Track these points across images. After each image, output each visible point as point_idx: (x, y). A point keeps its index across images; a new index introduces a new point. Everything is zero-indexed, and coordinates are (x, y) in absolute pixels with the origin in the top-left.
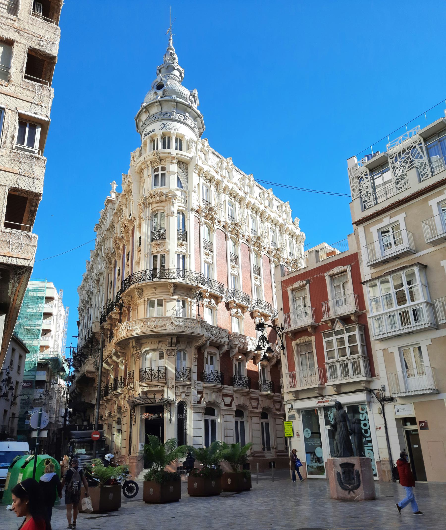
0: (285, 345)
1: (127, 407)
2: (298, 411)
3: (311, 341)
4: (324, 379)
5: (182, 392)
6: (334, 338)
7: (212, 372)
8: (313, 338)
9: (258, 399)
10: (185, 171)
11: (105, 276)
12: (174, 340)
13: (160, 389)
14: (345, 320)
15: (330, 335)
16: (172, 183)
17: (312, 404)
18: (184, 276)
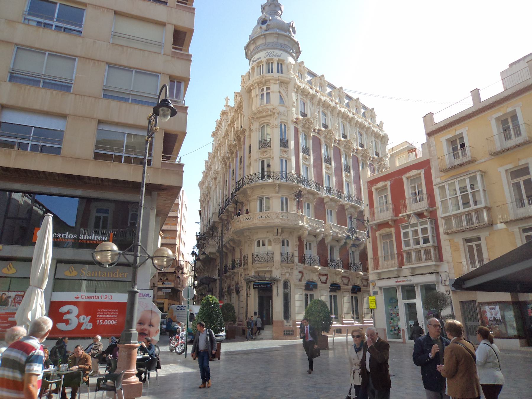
0: (370, 235)
1: (244, 284)
2: (380, 288)
3: (391, 232)
4: (401, 264)
5: (287, 272)
6: (410, 230)
8: (393, 230)
9: (348, 278)
14: (420, 215)
15: (406, 227)
16: (274, 99)
17: (391, 283)
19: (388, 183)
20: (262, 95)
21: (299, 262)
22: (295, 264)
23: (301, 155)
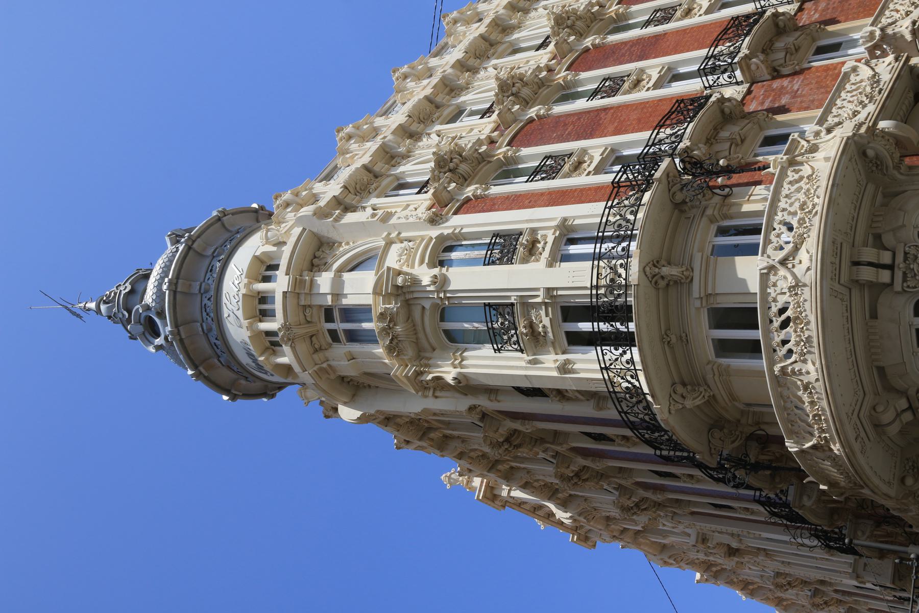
11: (714, 527)
20: (353, 336)
23: (558, 183)
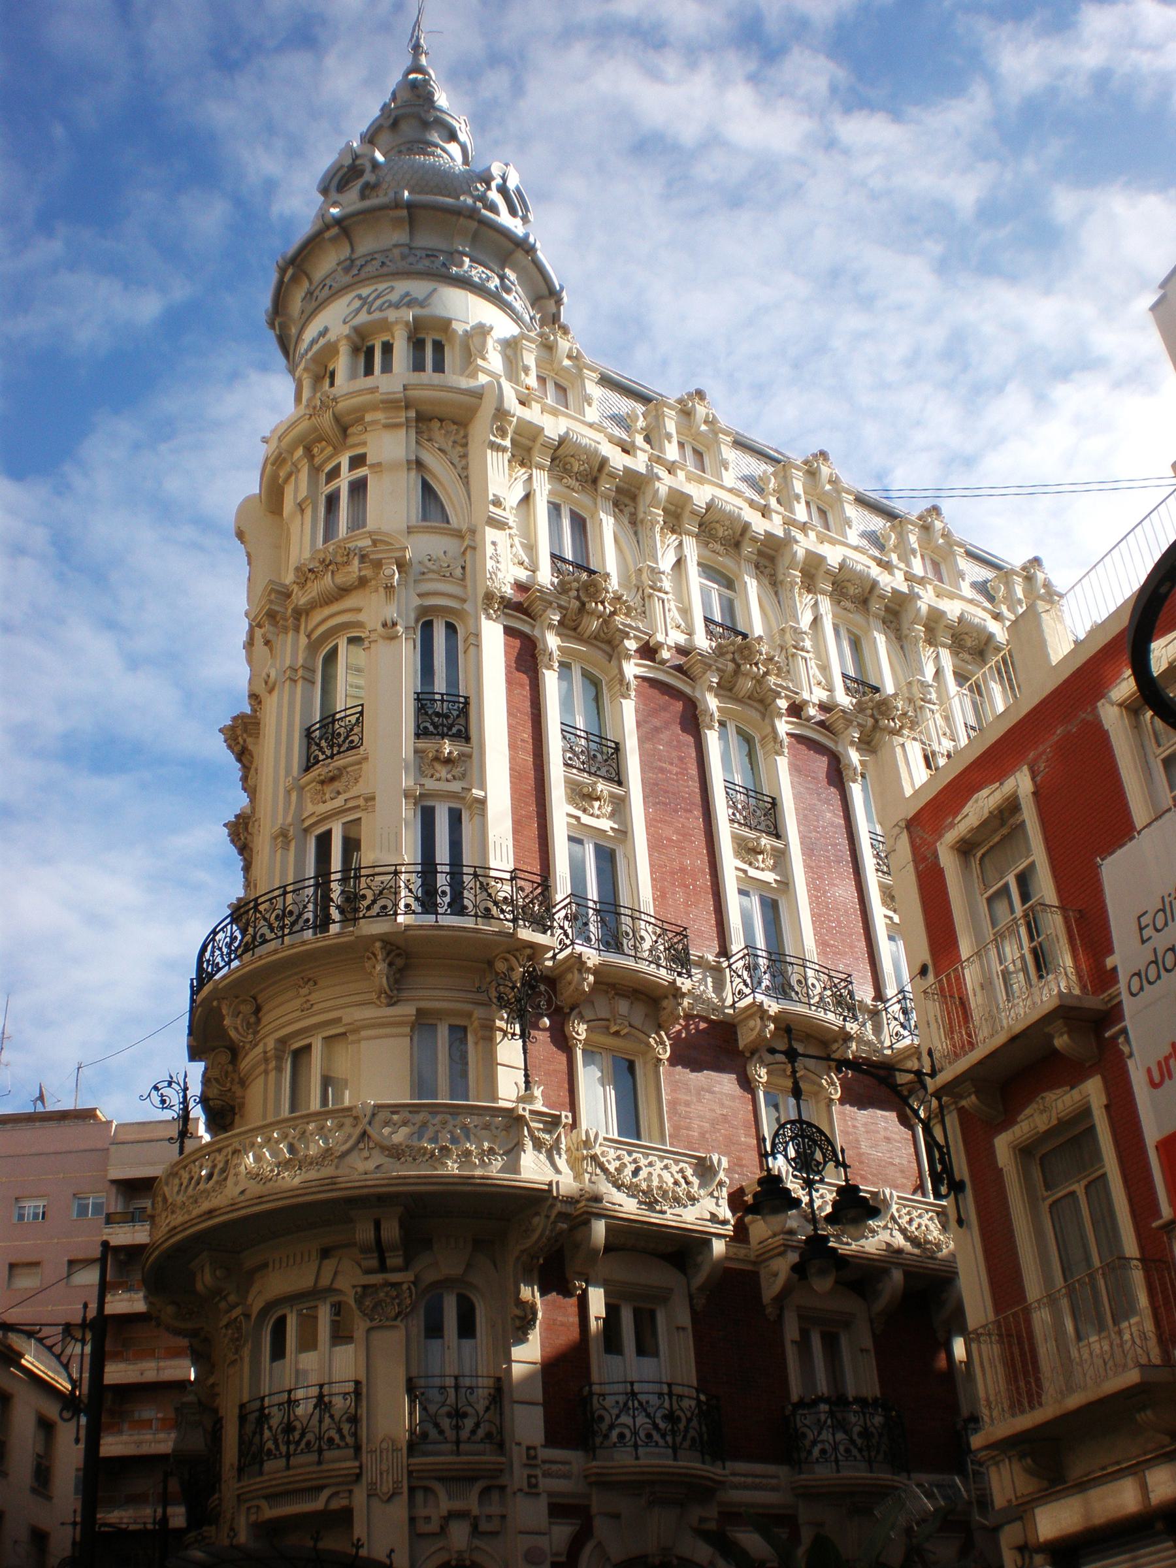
0: (961, 1170)
3: (1085, 1112)
5: (452, 1515)
7: (633, 1394)
8: (1093, 1090)
10: (455, 454)
12: (391, 1231)
13: (335, 1505)
16: (391, 506)
18: (457, 907)
19: (1021, 783)
21: (552, 1439)
22: (518, 1456)
